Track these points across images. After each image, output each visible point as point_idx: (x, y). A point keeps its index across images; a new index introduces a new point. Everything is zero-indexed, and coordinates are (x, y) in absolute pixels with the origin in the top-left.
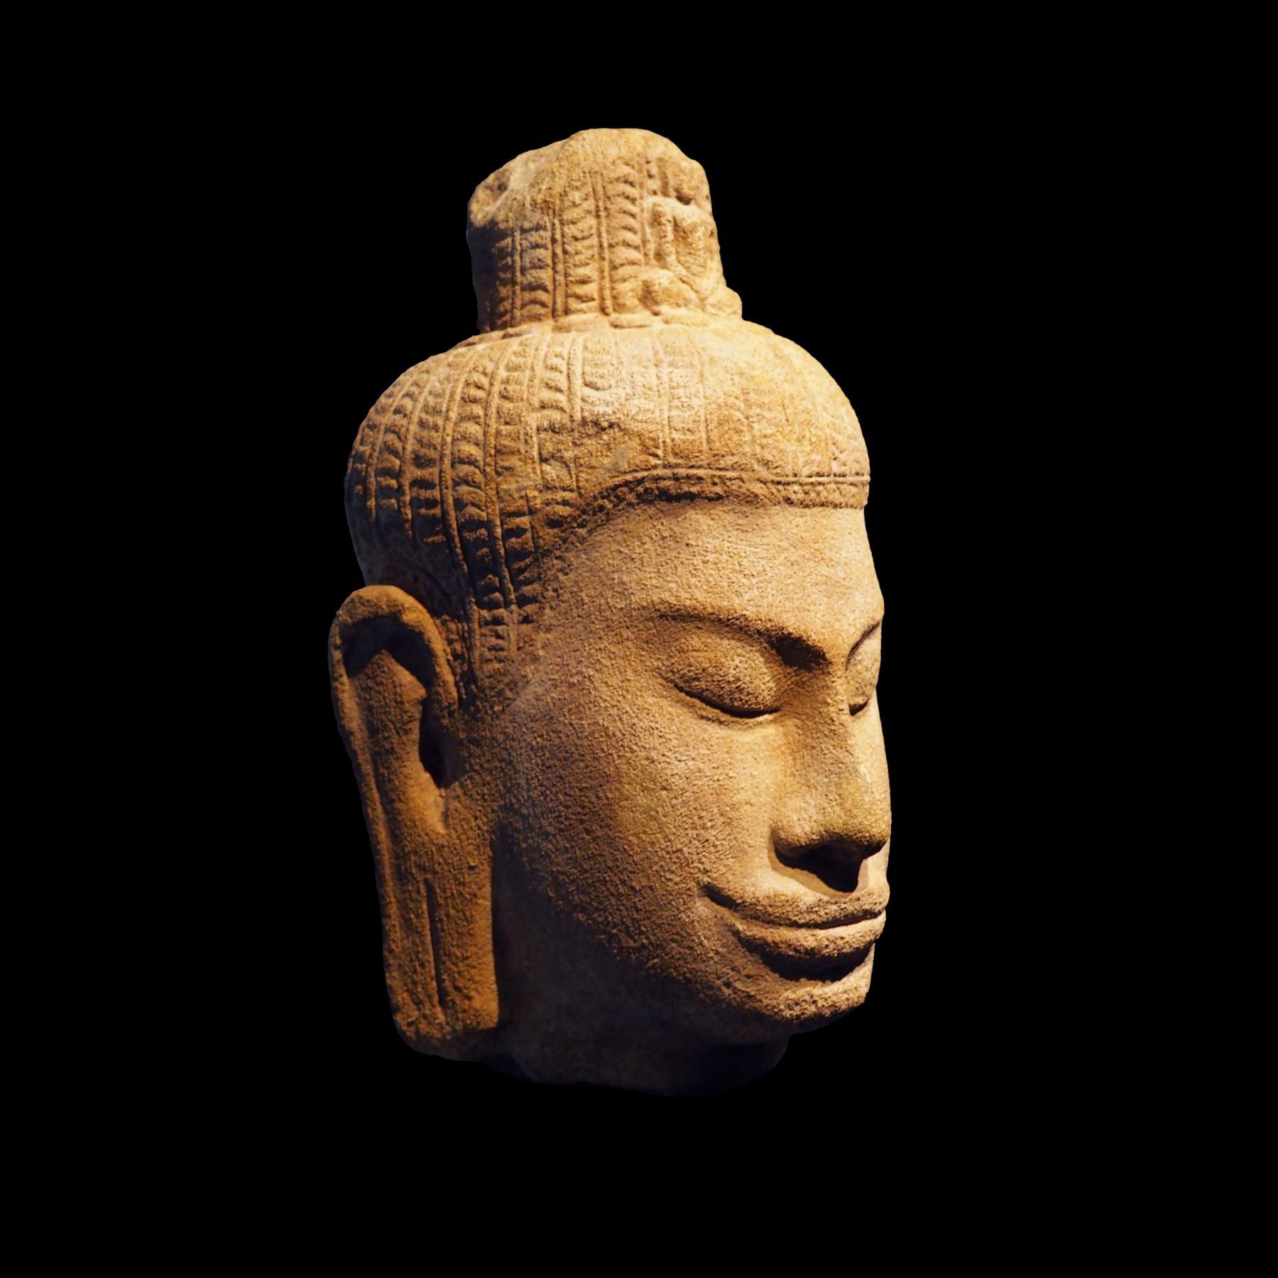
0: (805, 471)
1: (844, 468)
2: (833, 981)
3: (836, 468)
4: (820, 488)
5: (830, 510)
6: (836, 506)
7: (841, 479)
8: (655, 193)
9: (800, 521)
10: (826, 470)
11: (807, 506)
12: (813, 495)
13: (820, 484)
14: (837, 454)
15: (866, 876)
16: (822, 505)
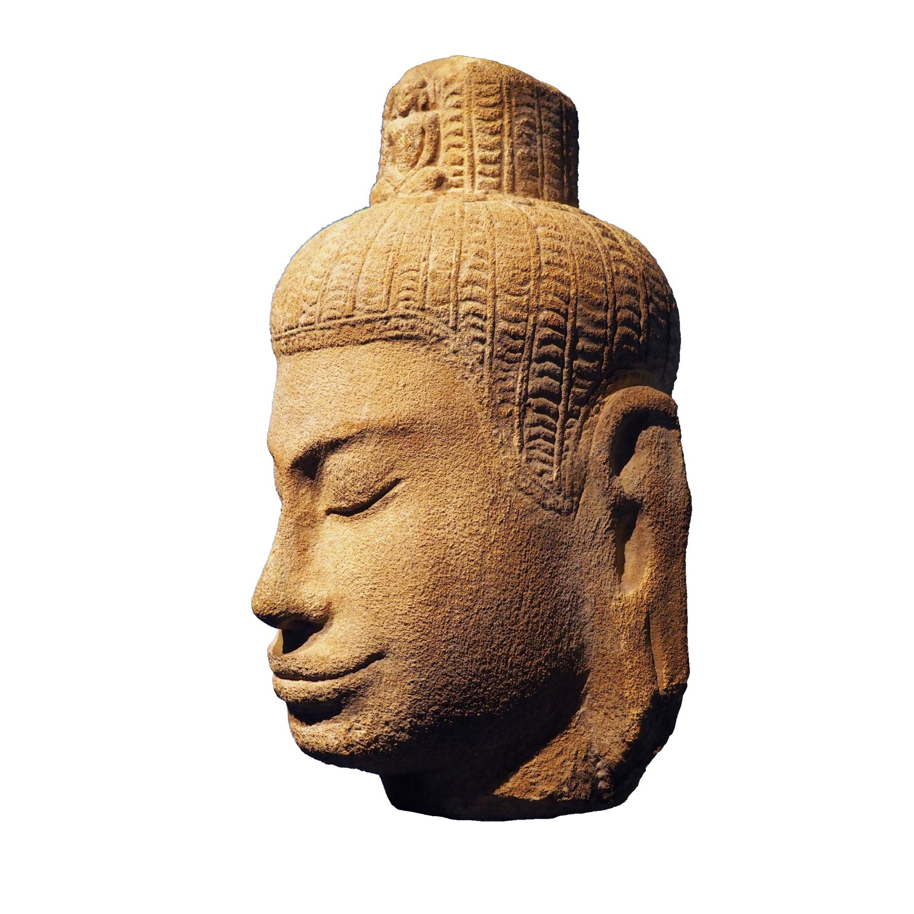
0: (284, 327)
1: (311, 319)
2: (307, 724)
3: (303, 319)
4: (292, 338)
5: (305, 354)
6: (310, 349)
7: (309, 327)
8: (395, 117)
9: (289, 364)
10: (294, 325)
11: (290, 354)
12: (290, 344)
13: (292, 335)
14: (305, 306)
15: (311, 645)
16: (299, 351)
